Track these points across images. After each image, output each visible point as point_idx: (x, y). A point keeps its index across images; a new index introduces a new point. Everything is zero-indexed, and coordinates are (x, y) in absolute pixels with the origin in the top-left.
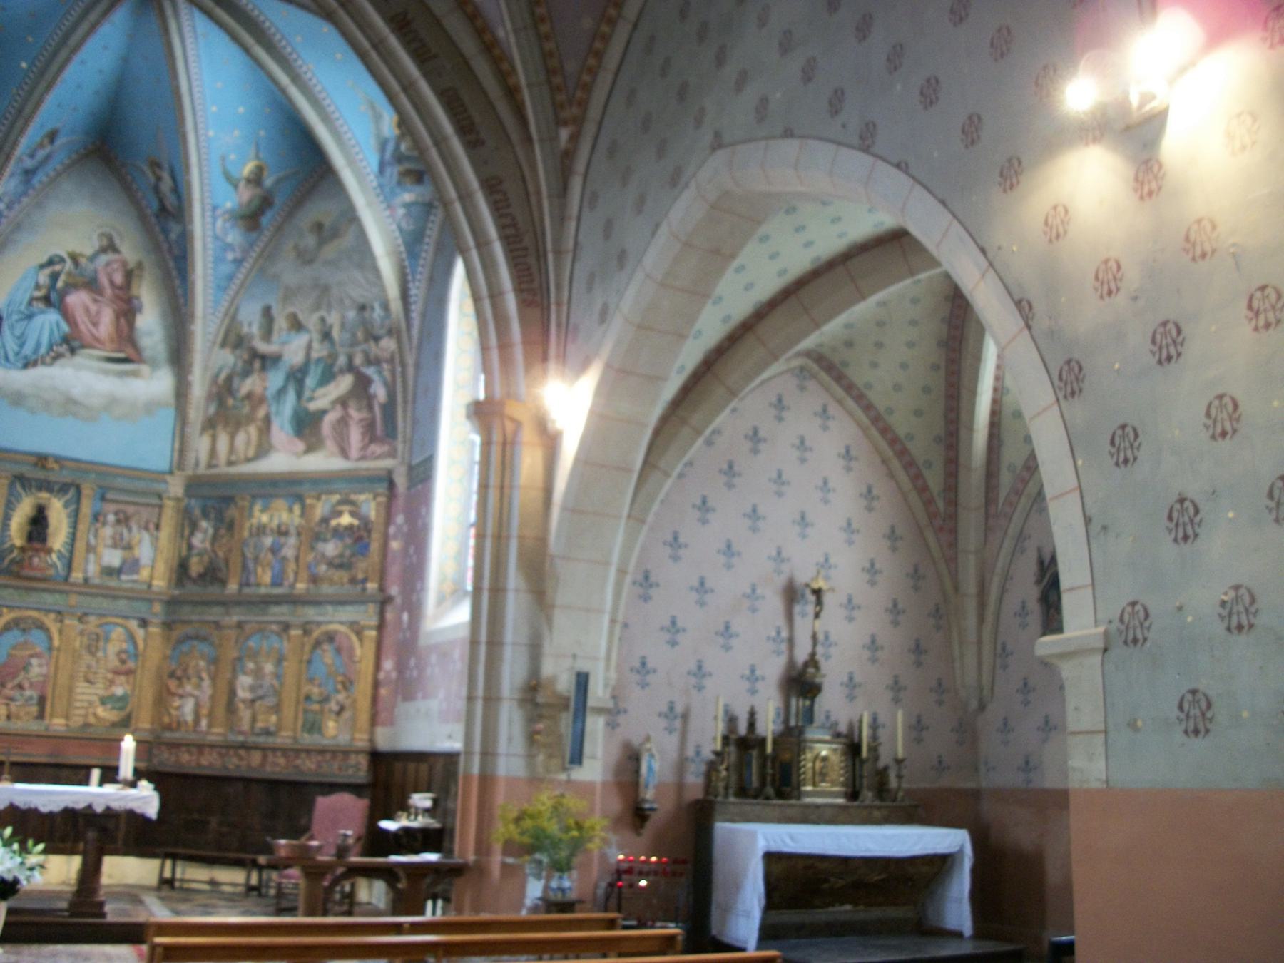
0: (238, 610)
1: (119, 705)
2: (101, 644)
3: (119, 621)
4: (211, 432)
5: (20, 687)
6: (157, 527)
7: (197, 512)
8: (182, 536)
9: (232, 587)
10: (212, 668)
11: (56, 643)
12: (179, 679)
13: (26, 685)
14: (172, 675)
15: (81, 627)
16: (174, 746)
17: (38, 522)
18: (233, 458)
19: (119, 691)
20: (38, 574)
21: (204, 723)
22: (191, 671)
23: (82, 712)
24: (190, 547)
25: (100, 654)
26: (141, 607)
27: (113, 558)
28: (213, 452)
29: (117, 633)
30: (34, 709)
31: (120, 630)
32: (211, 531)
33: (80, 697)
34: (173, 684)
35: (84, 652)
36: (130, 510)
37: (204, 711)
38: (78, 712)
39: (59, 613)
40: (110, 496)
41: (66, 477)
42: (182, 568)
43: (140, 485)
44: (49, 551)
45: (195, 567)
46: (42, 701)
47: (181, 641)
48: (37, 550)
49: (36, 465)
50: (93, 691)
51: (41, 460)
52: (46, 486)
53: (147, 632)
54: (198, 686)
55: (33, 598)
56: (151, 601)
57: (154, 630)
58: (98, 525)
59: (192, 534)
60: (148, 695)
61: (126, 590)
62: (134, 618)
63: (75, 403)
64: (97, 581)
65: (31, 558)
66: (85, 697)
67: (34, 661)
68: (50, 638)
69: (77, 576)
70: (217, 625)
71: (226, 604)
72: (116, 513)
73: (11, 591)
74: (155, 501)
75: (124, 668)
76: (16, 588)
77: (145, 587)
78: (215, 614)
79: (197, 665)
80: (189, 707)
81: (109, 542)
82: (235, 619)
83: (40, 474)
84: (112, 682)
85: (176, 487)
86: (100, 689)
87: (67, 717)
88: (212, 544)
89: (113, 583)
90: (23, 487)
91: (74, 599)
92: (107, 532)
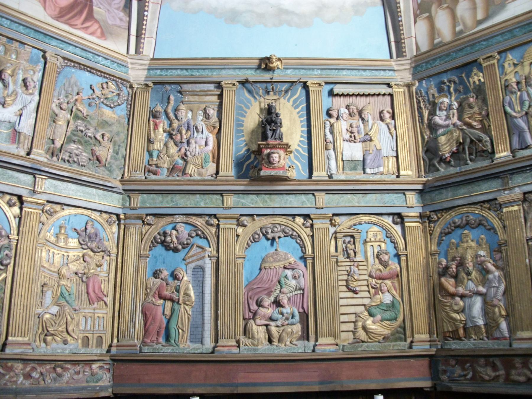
0: (518, 179)
1: (388, 315)
2: (359, 247)
3: (373, 219)
4: (427, 14)
5: (277, 303)
6: (393, 117)
7: (433, 91)
8: (422, 121)
9: (503, 154)
10: (498, 256)
11: (309, 251)
12: (456, 277)
13: (285, 301)
14: (444, 272)
15: (332, 230)
16: (465, 359)
17: (270, 120)
18: (458, 29)
19: (387, 298)
20: (280, 173)
21: (504, 325)
22: (470, 266)
23: (351, 327)
24: (433, 127)
25: (359, 257)
26: (394, 203)
27: (353, 151)
28: (433, 30)
29: (374, 232)
30: (297, 328)
31: (375, 228)
32: (456, 105)
33: (343, 310)
34: (449, 283)
35: (341, 258)
36: (361, 102)
37: (500, 310)
38: (344, 327)
39: (306, 216)
40: (336, 91)
41: (291, 75)
42: (430, 153)
43: (367, 76)
44: (286, 147)
45: (446, 148)
46: (304, 317)
47: (446, 233)
48: (274, 147)
49: (259, 67)
50: (360, 301)
51: (265, 64)
52: (269, 87)
53: (403, 229)
54: (484, 281)
55: (277, 203)
56: (403, 192)
57: (412, 224)
58: (333, 120)
59: (432, 113)
60: (420, 299)
61: (373, 182)
62: (389, 214)
63: (287, 12)
64: (342, 177)
65: (269, 155)
66: (352, 310)
67: (289, 273)
68: (303, 247)
69: (319, 174)
70: (493, 204)
71: (503, 174)
72: (348, 107)
73: (254, 197)
74: (384, 90)
75: (386, 272)
76: (258, 193)
77: (394, 177)
78: (486, 190)
79: (477, 256)
80: (478, 304)
81: (347, 136)
82: (518, 192)
83: (266, 76)
84: (378, 290)
85: (401, 74)
86: (364, 298)
87: (334, 335)
88: (460, 119)
89: (358, 175)
90: (250, 92)
91: (323, 199)
92: (342, 126)
